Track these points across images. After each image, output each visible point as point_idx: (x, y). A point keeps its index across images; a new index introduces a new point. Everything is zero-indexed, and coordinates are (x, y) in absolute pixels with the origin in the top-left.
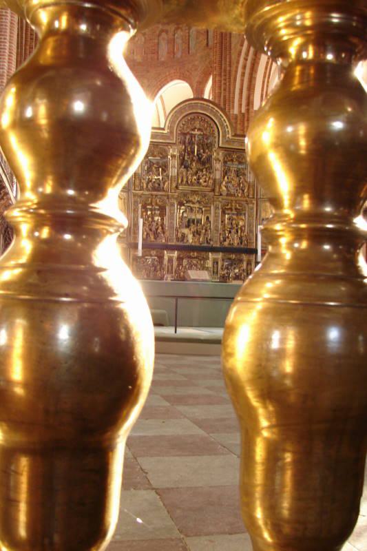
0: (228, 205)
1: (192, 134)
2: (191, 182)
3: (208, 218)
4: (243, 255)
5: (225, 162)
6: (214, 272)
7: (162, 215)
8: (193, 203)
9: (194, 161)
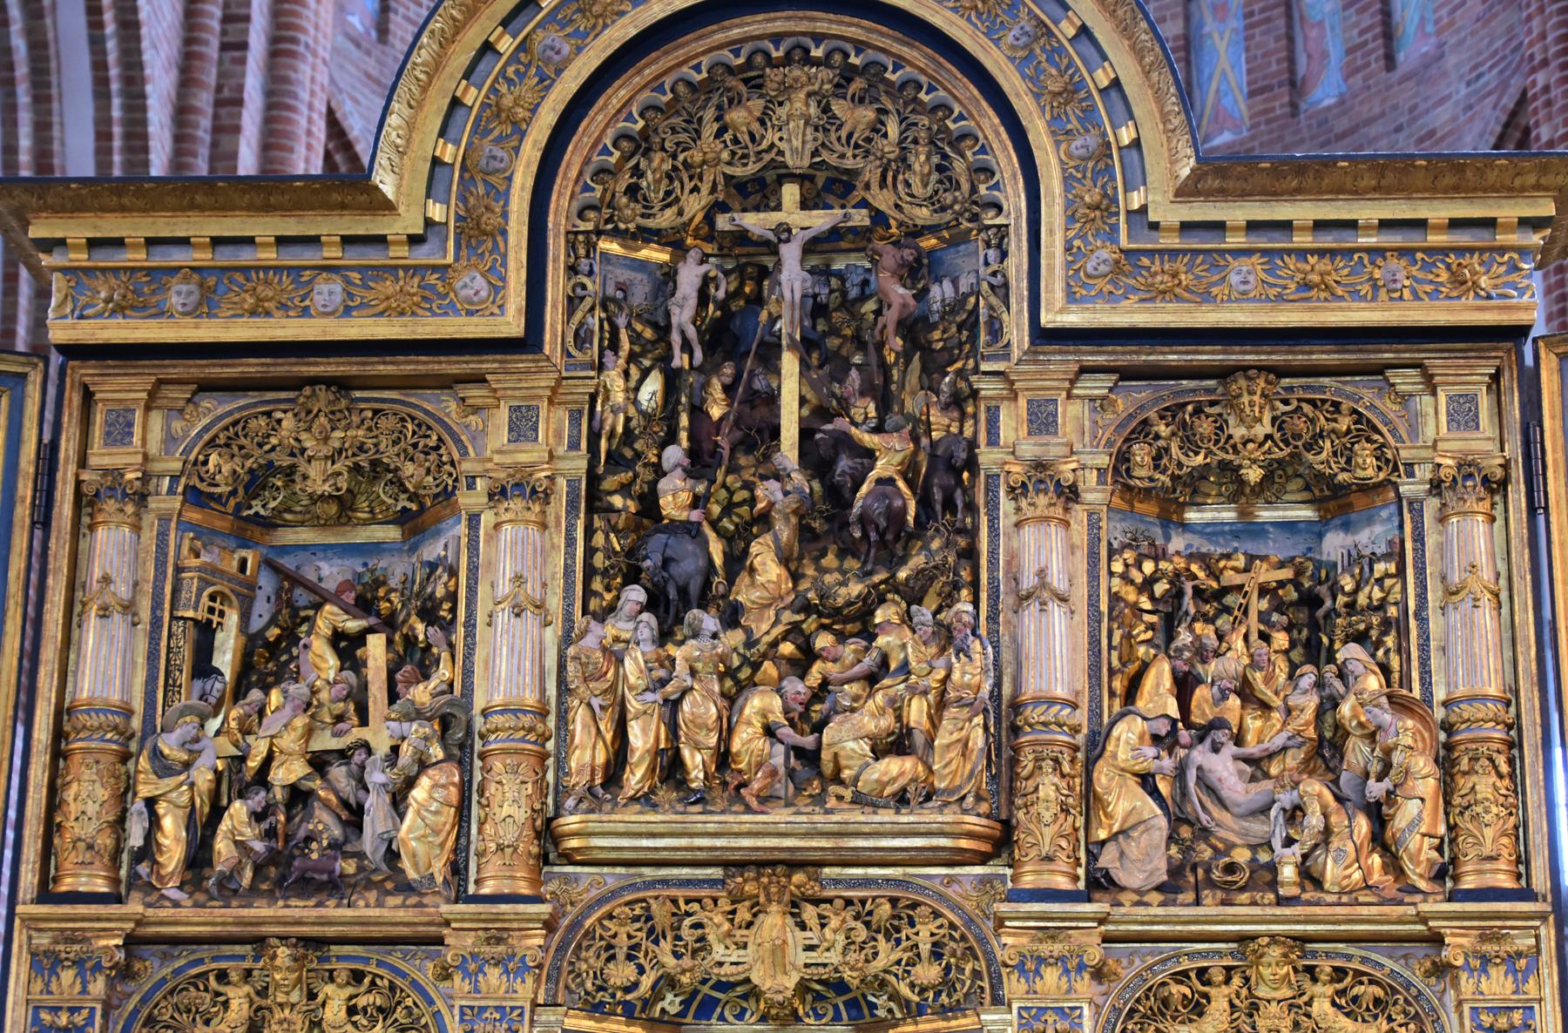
1: (742, 237)
2: (723, 758)
9: (764, 520)
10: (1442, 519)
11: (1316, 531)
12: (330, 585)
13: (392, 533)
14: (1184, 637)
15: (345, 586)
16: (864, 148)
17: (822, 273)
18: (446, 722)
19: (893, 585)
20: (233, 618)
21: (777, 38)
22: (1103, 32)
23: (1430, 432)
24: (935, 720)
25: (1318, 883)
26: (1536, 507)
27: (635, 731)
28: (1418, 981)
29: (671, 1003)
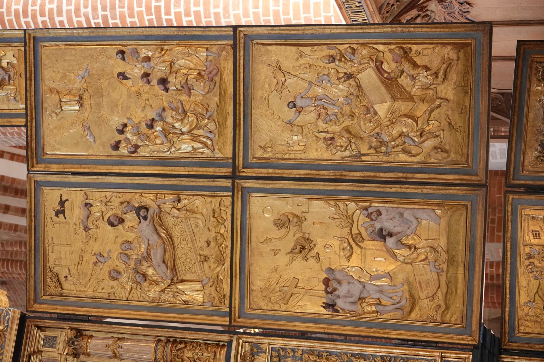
23: (55, 355)
26: (87, 319)
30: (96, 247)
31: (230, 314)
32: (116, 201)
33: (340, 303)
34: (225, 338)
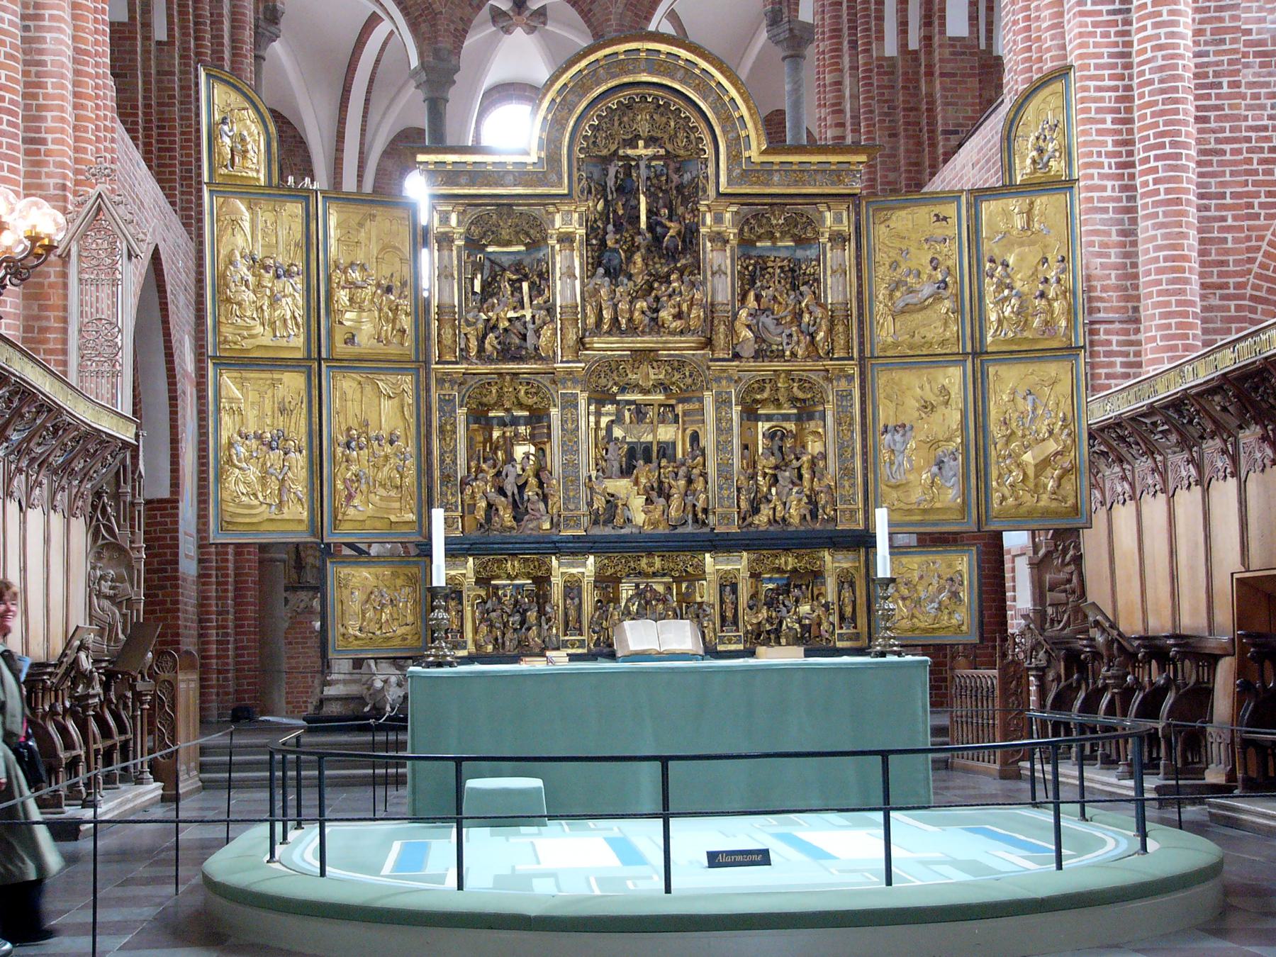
0: (762, 390)
1: (627, 157)
2: (630, 320)
3: (695, 438)
4: (827, 556)
5: (746, 243)
6: (723, 619)
7: (540, 441)
8: (645, 392)
9: (638, 248)
10: (832, 250)
11: (794, 249)
12: (506, 265)
13: (522, 248)
14: (759, 284)
15: (510, 266)
16: (664, 130)
17: (648, 167)
18: (548, 310)
19: (677, 269)
20: (479, 276)
21: (637, 95)
22: (739, 101)
23: (828, 223)
24: (690, 309)
25: (796, 356)
27: (604, 312)
28: (821, 382)
29: (615, 389)
30: (912, 250)
31: (872, 357)
32: (950, 263)
33: (888, 437)
34: (856, 355)
